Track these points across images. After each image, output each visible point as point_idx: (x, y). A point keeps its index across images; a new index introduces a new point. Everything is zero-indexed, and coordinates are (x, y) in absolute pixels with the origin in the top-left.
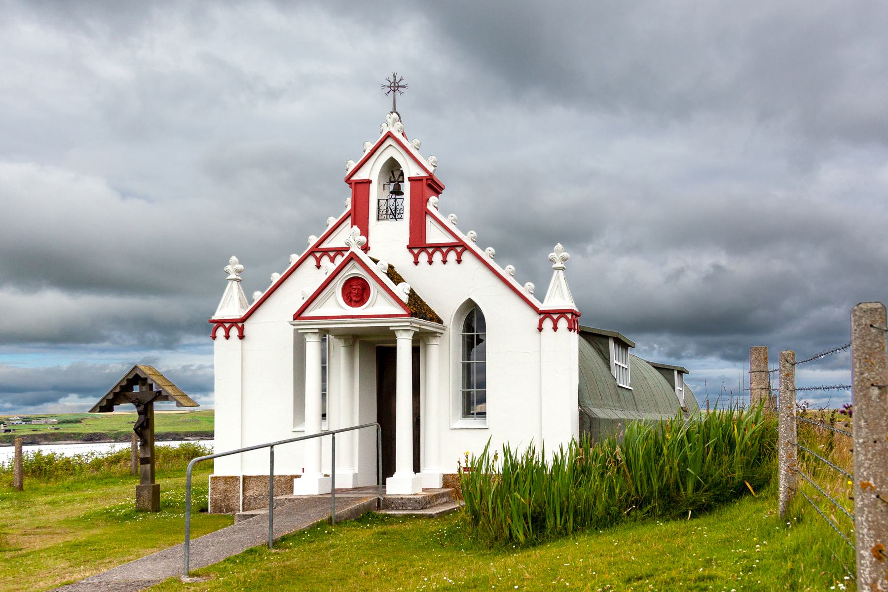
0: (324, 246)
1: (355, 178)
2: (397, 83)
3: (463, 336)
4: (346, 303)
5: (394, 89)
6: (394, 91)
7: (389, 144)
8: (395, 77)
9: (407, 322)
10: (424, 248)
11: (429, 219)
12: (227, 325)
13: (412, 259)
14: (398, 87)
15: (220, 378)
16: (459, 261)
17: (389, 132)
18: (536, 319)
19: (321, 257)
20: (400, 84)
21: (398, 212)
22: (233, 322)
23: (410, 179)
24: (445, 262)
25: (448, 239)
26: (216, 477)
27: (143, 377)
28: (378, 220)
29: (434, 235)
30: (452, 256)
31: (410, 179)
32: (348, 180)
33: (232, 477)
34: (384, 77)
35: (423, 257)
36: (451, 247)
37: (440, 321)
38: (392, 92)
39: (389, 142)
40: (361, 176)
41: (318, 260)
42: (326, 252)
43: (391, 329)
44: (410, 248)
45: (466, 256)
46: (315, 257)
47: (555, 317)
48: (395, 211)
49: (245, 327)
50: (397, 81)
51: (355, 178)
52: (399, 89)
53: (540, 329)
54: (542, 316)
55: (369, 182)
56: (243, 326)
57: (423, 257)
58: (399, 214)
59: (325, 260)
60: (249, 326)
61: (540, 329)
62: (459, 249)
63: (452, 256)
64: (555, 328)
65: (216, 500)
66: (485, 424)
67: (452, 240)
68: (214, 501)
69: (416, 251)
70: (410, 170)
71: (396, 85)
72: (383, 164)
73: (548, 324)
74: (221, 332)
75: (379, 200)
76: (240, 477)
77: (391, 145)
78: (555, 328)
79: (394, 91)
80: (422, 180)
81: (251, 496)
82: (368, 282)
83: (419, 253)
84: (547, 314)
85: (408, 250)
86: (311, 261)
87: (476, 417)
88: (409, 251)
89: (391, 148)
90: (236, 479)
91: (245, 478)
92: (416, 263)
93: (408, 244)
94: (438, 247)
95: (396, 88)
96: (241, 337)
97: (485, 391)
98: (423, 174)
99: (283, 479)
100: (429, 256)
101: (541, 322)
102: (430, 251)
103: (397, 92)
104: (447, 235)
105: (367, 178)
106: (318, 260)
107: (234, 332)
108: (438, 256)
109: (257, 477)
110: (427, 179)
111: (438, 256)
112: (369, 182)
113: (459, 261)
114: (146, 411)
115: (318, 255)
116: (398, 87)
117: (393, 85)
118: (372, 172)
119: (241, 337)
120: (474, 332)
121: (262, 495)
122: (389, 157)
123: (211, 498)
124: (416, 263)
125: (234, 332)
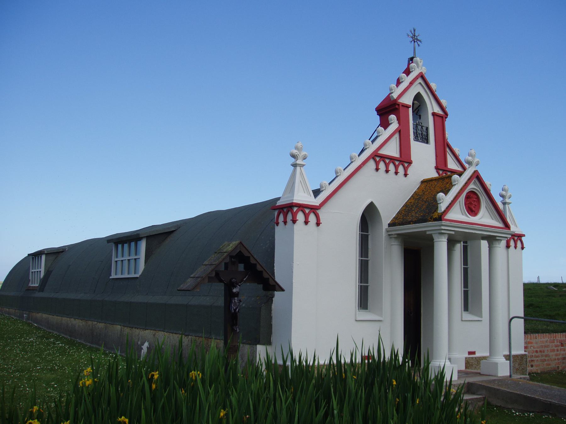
0: (381, 152)
8: (414, 30)
12: (307, 211)
15: (298, 263)
22: (314, 209)
23: (434, 114)
25: (458, 168)
27: (246, 255)
31: (434, 114)
41: (377, 164)
42: (383, 157)
43: (428, 233)
46: (375, 160)
47: (516, 238)
53: (508, 246)
55: (407, 107)
59: (382, 166)
61: (508, 246)
66: (482, 317)
70: (432, 107)
73: (512, 243)
93: (435, 165)
96: (318, 224)
98: (441, 112)
104: (458, 165)
107: (312, 218)
115: (378, 159)
118: (408, 100)
119: (318, 224)
125: (312, 218)
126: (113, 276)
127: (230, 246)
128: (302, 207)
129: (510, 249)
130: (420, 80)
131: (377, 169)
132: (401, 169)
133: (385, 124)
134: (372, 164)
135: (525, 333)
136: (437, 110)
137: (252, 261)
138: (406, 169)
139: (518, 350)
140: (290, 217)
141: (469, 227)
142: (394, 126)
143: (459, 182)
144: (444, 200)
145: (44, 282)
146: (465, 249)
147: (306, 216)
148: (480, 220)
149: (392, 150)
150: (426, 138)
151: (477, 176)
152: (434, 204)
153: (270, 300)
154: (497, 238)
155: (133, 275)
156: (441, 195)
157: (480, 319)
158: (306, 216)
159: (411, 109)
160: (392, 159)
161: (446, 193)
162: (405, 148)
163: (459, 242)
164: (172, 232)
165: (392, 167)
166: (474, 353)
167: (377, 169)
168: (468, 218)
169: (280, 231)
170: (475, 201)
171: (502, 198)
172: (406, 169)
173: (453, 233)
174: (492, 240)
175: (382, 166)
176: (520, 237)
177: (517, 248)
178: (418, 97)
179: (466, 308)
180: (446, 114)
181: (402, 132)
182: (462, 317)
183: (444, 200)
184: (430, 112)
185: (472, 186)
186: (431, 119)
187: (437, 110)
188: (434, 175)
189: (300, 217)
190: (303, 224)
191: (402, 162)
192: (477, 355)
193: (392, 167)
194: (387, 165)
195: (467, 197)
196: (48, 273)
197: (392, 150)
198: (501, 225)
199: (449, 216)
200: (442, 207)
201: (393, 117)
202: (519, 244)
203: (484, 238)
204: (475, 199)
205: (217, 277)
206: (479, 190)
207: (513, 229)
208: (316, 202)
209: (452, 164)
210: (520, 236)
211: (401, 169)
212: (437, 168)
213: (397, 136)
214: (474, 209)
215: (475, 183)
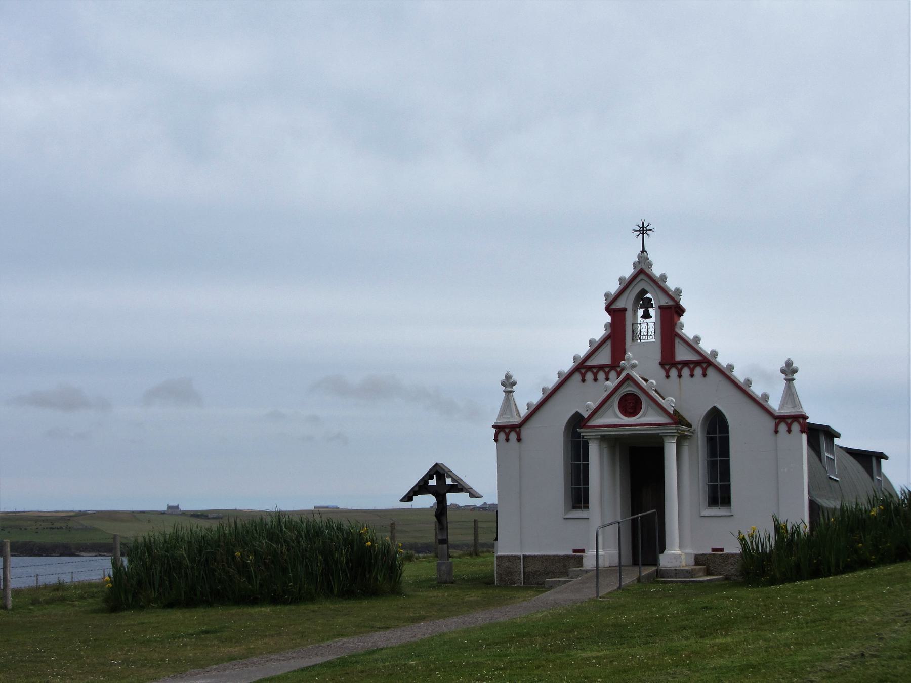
0: (589, 363)
1: (613, 307)
2: (646, 228)
3: (707, 437)
4: (622, 414)
5: (643, 232)
6: (643, 234)
7: (641, 278)
9: (673, 429)
10: (674, 364)
11: (677, 341)
12: (507, 430)
13: (663, 373)
14: (647, 230)
16: (704, 375)
17: (641, 268)
18: (771, 424)
19: (586, 372)
20: (648, 228)
21: (650, 334)
24: (692, 376)
26: (500, 556)
28: (633, 340)
29: (682, 354)
30: (698, 371)
31: (660, 307)
32: (608, 309)
33: (515, 556)
34: (635, 223)
35: (674, 373)
36: (697, 363)
37: (690, 426)
38: (641, 235)
39: (642, 276)
40: (620, 304)
41: (583, 376)
42: (590, 368)
44: (662, 364)
45: (711, 372)
46: (581, 373)
47: (789, 421)
48: (648, 333)
49: (522, 431)
50: (645, 226)
51: (613, 307)
52: (648, 232)
53: (776, 432)
54: (777, 421)
55: (625, 310)
56: (520, 430)
57: (674, 373)
58: (643, 336)
59: (589, 376)
60: (525, 432)
61: (776, 432)
62: (704, 365)
63: (698, 371)
64: (789, 431)
65: (501, 574)
67: (695, 357)
68: (499, 574)
69: (667, 367)
71: (645, 229)
72: (636, 294)
73: (783, 427)
74: (502, 436)
75: (633, 324)
76: (521, 556)
77: (642, 279)
78: (789, 431)
79: (643, 234)
80: (671, 308)
81: (530, 572)
82: (639, 396)
83: (670, 369)
85: (660, 367)
86: (577, 377)
87: (721, 506)
88: (662, 367)
89: (643, 281)
90: (517, 557)
91: (524, 556)
92: (668, 377)
93: (660, 360)
94: (686, 364)
95: (645, 232)
96: (519, 440)
97: (730, 484)
98: (671, 303)
99: (556, 558)
100: (678, 371)
101: (777, 426)
102: (680, 367)
103: (645, 235)
105: (623, 307)
106: (583, 376)
107: (513, 436)
108: (686, 372)
109: (535, 556)
110: (675, 307)
111: (686, 372)
112: (625, 310)
113: (704, 375)
114: (441, 500)
115: (583, 371)
116: (647, 230)
117: (642, 229)
119: (519, 440)
120: (717, 434)
121: (539, 571)
122: (640, 289)
123: (497, 573)
124: (668, 377)
125: (513, 436)
129: (778, 435)
131: (583, 381)
134: (577, 377)
136: (664, 301)
141: (608, 430)
148: (640, 419)
150: (653, 334)
154: (661, 434)
157: (730, 514)
160: (601, 368)
166: (722, 550)
167: (583, 381)
168: (622, 421)
170: (630, 403)
171: (784, 375)
173: (599, 437)
175: (589, 376)
177: (791, 432)
182: (700, 513)
186: (659, 311)
190: (504, 441)
192: (726, 552)
197: (604, 358)
199: (598, 421)
204: (629, 401)
206: (633, 390)
208: (515, 420)
211: (613, 374)
213: (609, 343)
214: (629, 410)
215: (629, 385)
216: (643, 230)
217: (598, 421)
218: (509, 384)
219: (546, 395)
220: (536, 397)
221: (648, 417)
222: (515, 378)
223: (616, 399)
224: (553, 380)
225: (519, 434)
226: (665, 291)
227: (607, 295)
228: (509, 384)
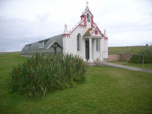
0: (81, 24)
12: (67, 35)
22: (69, 35)
23: (91, 17)
31: (91, 17)
41: (80, 26)
42: (81, 25)
53: (105, 40)
59: (81, 27)
60: (70, 35)
61: (105, 40)
70: (90, 16)
73: (106, 39)
84: (106, 38)
107: (68, 36)
118: (86, 14)
125: (68, 36)
126: (39, 48)
127: (54, 42)
128: (67, 34)
130: (88, 11)
131: (80, 27)
132: (85, 27)
133: (82, 19)
134: (79, 26)
135: (108, 54)
136: (91, 16)
137: (58, 44)
138: (85, 27)
139: (107, 57)
140: (65, 36)
142: (83, 19)
143: (94, 29)
144: (91, 32)
145: (28, 50)
146: (97, 41)
147: (67, 36)
149: (83, 24)
151: (97, 28)
152: (89, 33)
153: (62, 50)
155: (42, 48)
156: (90, 31)
158: (67, 36)
159: (86, 16)
160: (83, 25)
161: (91, 31)
162: (85, 23)
163: (95, 39)
164: (49, 39)
165: (83, 27)
169: (63, 38)
172: (85, 27)
174: (100, 39)
175: (81, 27)
176: (107, 38)
178: (88, 14)
179: (97, 50)
180: (93, 17)
181: (85, 21)
183: (91, 32)
184: (90, 17)
185: (96, 30)
186: (90, 18)
187: (91, 16)
188: (91, 28)
189: (66, 36)
191: (85, 26)
193: (83, 27)
194: (82, 26)
195: (95, 31)
196: (29, 48)
197: (83, 24)
198: (102, 36)
199: (92, 35)
200: (90, 33)
201: (83, 18)
202: (107, 39)
203: (99, 38)
205: (52, 46)
207: (106, 37)
209: (94, 26)
210: (107, 38)
211: (85, 27)
212: (91, 27)
216: (87, 3)
217: (92, 35)
218: (66, 26)
219: (73, 29)
220: (72, 30)
221: (99, 35)
222: (67, 25)
223: (95, 31)
224: (75, 27)
225: (69, 36)
226: (92, 15)
227: (83, 13)
228: (66, 26)
